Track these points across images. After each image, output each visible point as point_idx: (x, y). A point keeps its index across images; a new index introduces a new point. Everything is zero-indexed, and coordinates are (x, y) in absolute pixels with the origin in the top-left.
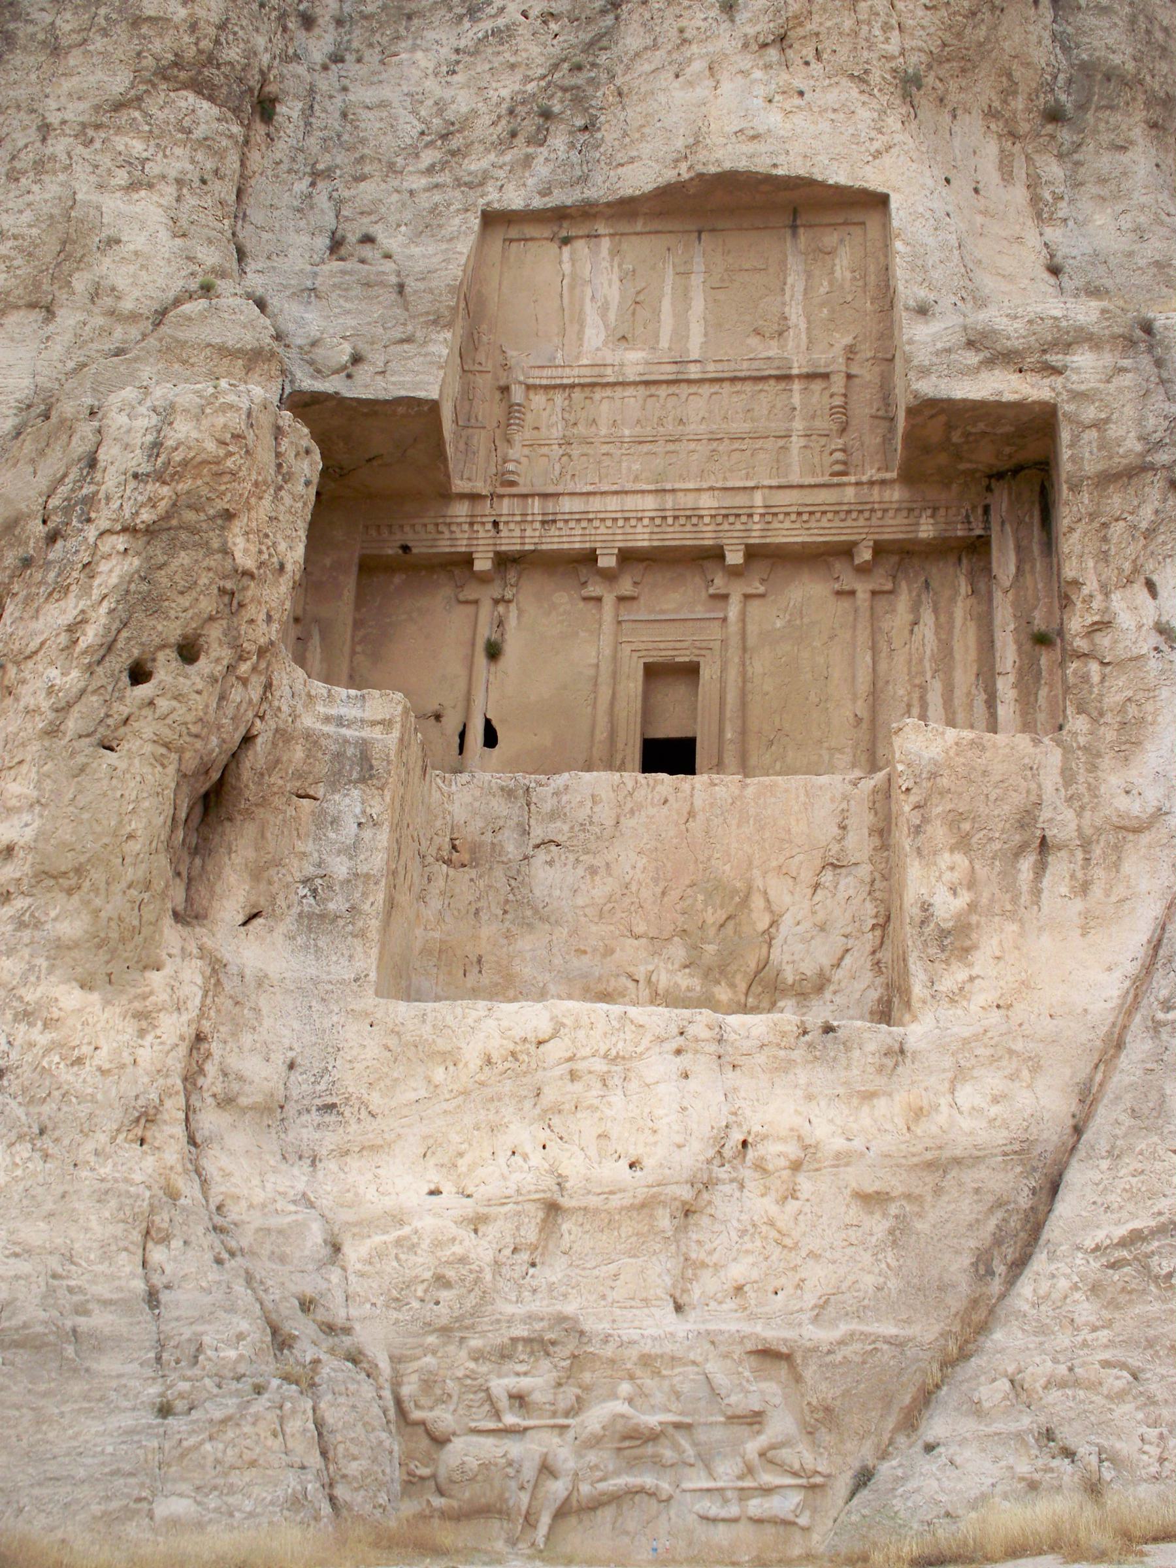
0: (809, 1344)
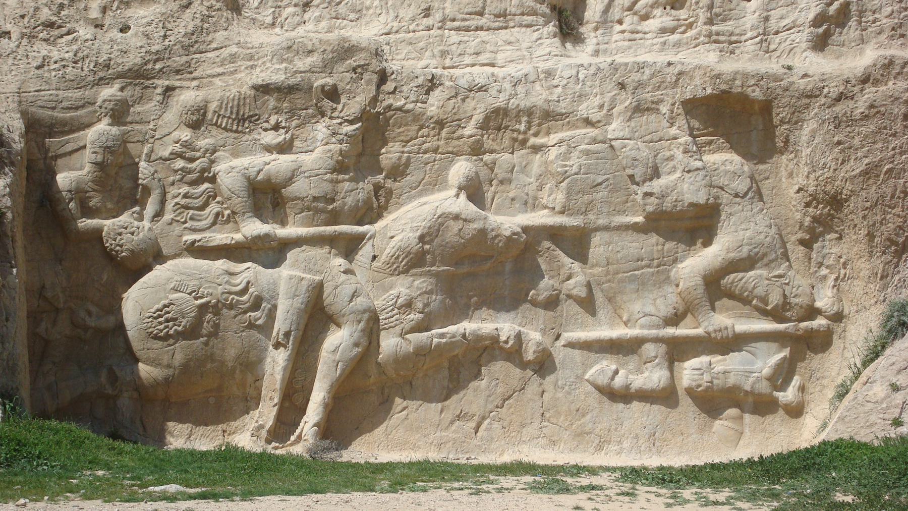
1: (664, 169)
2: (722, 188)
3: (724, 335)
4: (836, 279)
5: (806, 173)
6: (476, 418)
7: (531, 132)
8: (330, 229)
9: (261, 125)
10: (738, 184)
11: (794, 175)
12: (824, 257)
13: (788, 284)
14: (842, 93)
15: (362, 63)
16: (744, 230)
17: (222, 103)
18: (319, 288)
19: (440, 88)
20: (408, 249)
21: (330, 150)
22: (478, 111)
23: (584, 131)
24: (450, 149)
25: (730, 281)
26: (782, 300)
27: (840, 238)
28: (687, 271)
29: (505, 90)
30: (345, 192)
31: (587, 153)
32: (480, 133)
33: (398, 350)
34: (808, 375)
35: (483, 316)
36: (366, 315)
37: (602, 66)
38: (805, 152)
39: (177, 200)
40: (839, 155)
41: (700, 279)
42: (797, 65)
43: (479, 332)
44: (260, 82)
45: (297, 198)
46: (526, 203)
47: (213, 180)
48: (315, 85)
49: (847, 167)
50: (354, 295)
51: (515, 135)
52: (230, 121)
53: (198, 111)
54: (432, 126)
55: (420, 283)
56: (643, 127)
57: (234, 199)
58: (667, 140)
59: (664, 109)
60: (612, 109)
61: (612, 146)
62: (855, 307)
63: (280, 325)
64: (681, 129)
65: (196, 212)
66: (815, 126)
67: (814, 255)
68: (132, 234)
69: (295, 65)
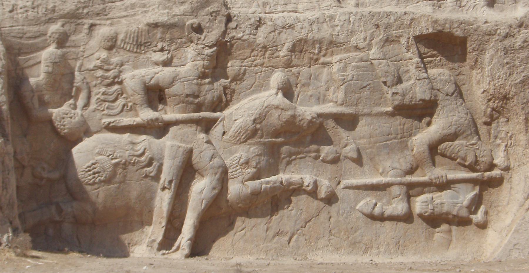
0: (484, 27)
1: (404, 78)
2: (438, 90)
3: (441, 181)
4: (506, 146)
5: (488, 82)
6: (289, 234)
7: (322, 54)
8: (196, 115)
9: (152, 49)
10: (448, 88)
11: (481, 82)
12: (498, 133)
13: (478, 149)
14: (508, 33)
15: (216, 10)
16: (452, 116)
17: (127, 35)
18: (190, 152)
19: (264, 26)
20: (247, 128)
21: (197, 65)
22: (289, 41)
23: (355, 54)
24: (271, 64)
25: (444, 147)
26: (474, 159)
27: (508, 121)
28: (418, 141)
29: (306, 27)
30: (206, 91)
31: (357, 67)
32: (290, 54)
33: (240, 192)
34: (489, 205)
35: (292, 170)
36: (220, 170)
37: (364, 14)
38: (487, 69)
39: (98, 96)
40: (507, 71)
41: (426, 146)
42: (479, 16)
43: (291, 180)
44: (152, 21)
45: (176, 95)
46: (319, 99)
47: (121, 83)
48: (187, 23)
49: (512, 78)
50: (212, 157)
51: (312, 55)
52: (132, 46)
53: (112, 39)
54: (260, 49)
55: (254, 149)
56: (391, 52)
57: (135, 96)
58: (405, 60)
59: (403, 41)
60: (372, 40)
61: (372, 63)
62: (517, 163)
63: (165, 177)
64: (414, 53)
65: (111, 104)
66: (493, 53)
67: (492, 132)
68: (71, 118)
69: (174, 11)
